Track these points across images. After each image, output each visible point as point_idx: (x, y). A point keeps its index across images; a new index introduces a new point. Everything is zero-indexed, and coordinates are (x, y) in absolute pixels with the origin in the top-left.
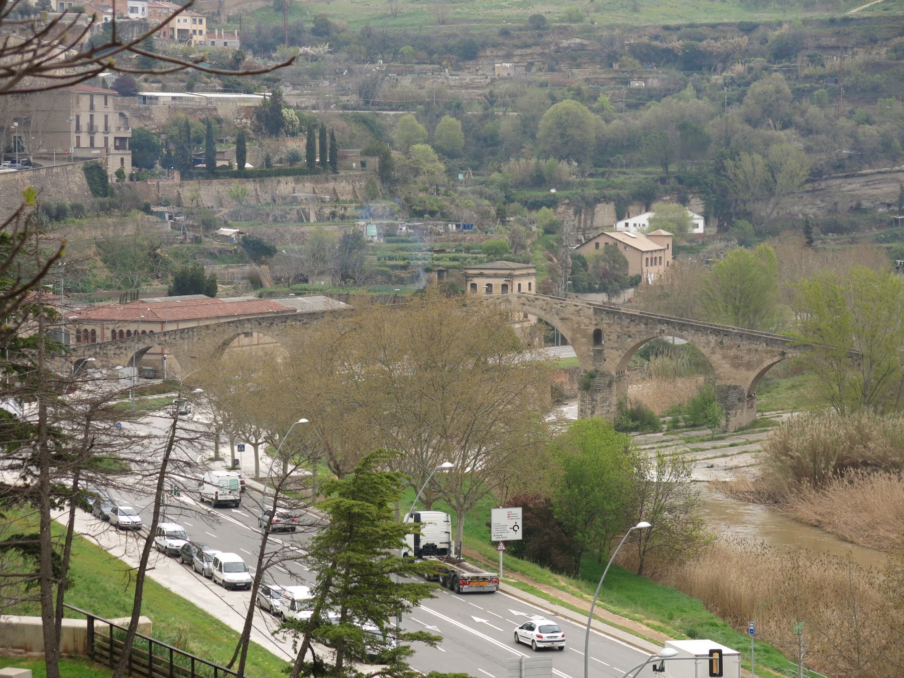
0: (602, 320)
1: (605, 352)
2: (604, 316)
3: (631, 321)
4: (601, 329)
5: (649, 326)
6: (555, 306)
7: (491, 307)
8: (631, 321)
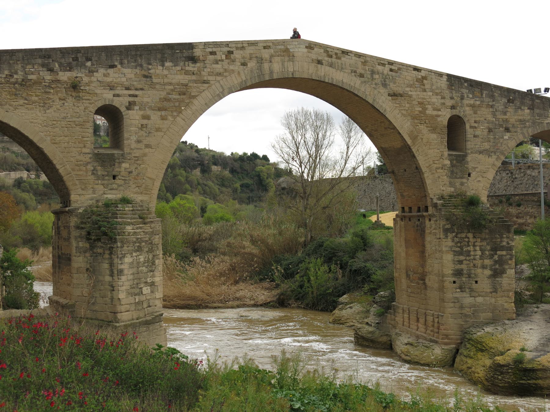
0: (462, 98)
1: (469, 158)
2: (465, 91)
3: (509, 101)
4: (461, 115)
5: (537, 111)
6: (380, 68)
7: (252, 64)
8: (509, 101)
